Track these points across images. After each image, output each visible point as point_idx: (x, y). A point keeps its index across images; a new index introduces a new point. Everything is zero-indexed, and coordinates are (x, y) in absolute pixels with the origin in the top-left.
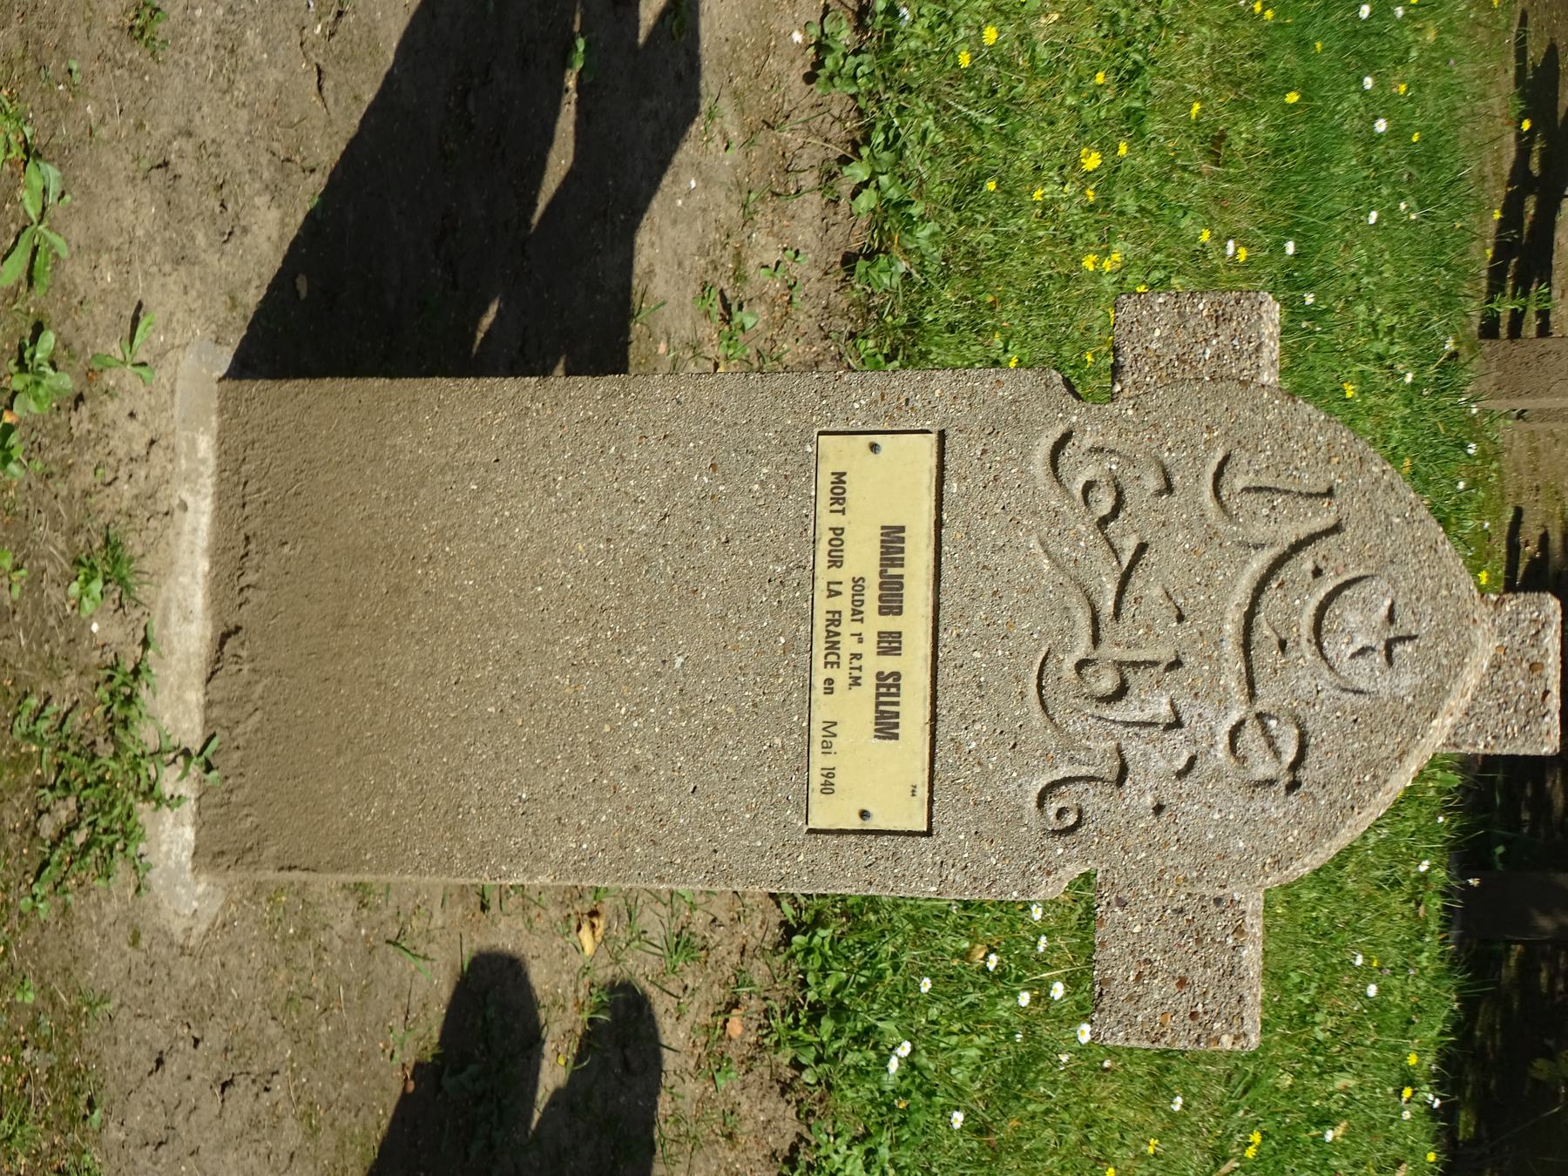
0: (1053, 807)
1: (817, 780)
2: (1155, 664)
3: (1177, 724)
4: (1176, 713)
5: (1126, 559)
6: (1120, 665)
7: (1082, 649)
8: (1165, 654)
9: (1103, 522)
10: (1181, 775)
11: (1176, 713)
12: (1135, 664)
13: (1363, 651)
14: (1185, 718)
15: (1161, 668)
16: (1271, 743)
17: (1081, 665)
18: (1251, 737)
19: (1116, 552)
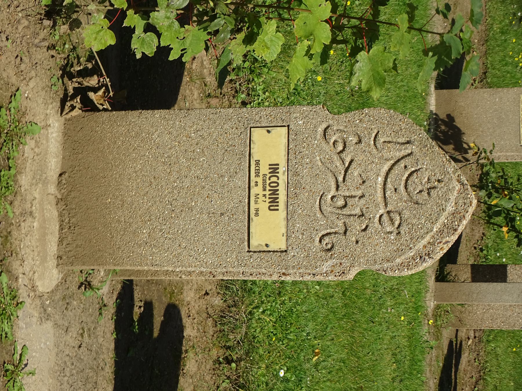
0: (327, 240)
1: (253, 212)
2: (355, 197)
3: (363, 215)
4: (362, 212)
5: (347, 165)
6: (345, 197)
7: (333, 192)
8: (359, 193)
9: (339, 153)
10: (365, 230)
11: (362, 212)
12: (349, 197)
13: (421, 191)
14: (364, 212)
15: (358, 197)
16: (392, 220)
17: (333, 198)
18: (385, 218)
19: (344, 164)
